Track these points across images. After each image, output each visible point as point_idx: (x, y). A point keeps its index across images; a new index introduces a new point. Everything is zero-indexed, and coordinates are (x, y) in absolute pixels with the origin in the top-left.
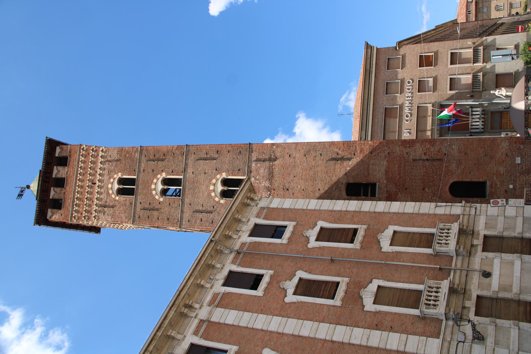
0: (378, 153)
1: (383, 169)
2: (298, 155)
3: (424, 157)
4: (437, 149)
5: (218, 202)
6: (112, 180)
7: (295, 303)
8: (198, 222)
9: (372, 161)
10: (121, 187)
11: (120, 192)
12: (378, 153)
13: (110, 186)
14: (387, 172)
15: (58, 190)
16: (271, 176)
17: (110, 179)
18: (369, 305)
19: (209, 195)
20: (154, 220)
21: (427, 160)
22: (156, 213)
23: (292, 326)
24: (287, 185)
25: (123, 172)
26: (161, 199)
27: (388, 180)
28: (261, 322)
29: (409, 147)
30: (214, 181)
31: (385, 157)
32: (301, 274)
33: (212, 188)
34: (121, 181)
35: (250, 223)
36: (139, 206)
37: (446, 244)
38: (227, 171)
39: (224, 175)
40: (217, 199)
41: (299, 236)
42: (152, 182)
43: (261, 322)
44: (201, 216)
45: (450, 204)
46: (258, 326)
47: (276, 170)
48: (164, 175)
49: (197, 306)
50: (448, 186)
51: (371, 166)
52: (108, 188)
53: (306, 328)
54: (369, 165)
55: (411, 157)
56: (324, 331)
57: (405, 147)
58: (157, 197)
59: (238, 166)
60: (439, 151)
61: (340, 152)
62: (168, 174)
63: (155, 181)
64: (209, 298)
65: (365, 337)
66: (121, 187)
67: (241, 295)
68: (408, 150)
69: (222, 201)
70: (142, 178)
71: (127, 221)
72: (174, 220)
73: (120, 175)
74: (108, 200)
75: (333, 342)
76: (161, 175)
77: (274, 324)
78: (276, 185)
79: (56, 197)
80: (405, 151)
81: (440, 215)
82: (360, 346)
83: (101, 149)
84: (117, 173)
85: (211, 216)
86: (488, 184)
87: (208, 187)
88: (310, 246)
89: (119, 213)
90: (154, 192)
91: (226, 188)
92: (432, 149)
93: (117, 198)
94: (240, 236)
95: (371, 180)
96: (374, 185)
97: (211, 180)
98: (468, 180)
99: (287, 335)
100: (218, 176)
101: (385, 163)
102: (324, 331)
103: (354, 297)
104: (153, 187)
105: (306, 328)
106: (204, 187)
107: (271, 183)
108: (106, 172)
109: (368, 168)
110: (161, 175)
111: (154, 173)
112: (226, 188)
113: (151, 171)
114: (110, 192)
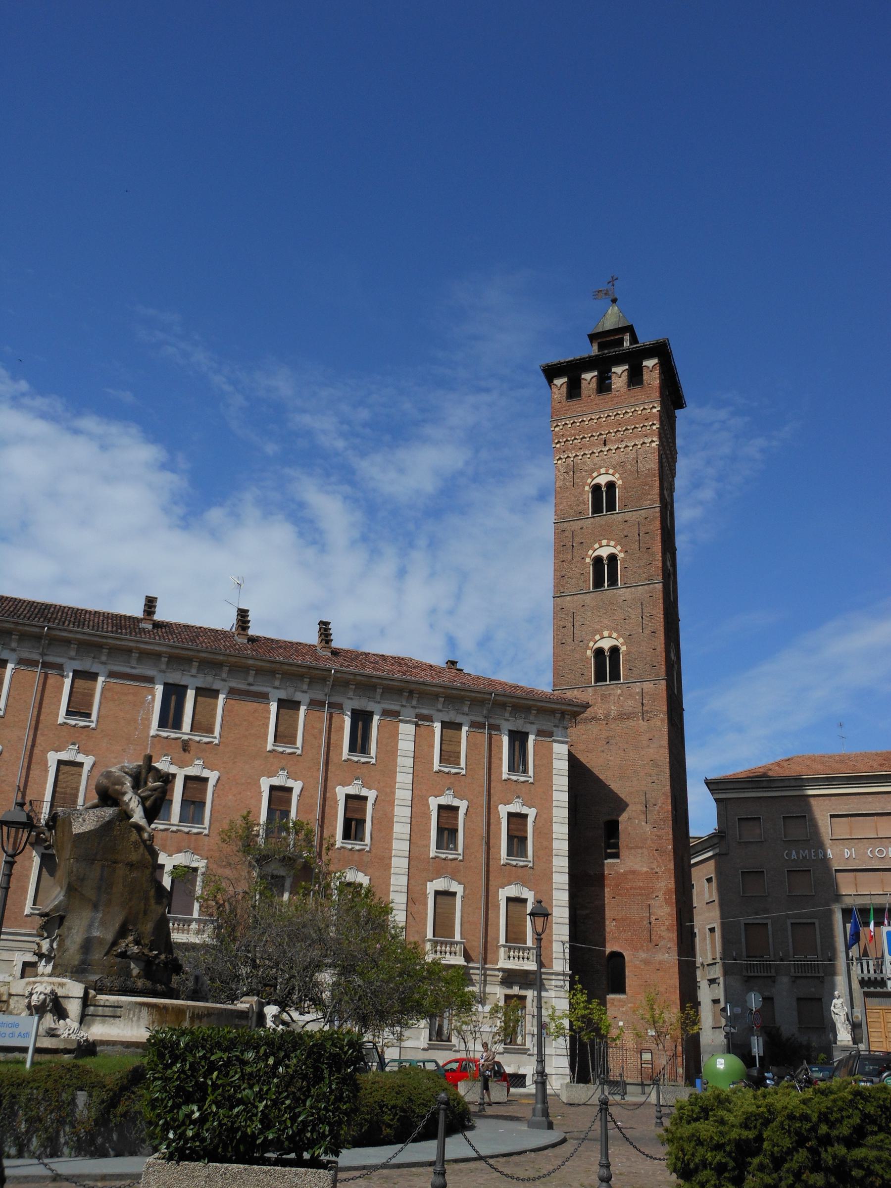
0: (656, 859)
1: (637, 867)
2: (651, 751)
3: (653, 918)
4: (663, 934)
5: (587, 647)
6: (611, 471)
7: (429, 808)
8: (562, 623)
9: (645, 851)
10: (604, 489)
11: (596, 488)
12: (656, 859)
13: (603, 471)
14: (633, 872)
15: (594, 384)
16: (624, 717)
17: (613, 467)
18: (432, 887)
19: (597, 632)
20: (561, 556)
21: (650, 923)
22: (569, 556)
23: (402, 813)
24: (612, 741)
25: (624, 488)
26: (588, 560)
27: (625, 874)
28: (404, 779)
29: (665, 898)
30: (615, 635)
31: (652, 869)
32: (463, 805)
33: (606, 634)
34: (611, 486)
35: (528, 725)
36: (576, 525)
37: (509, 957)
38: (628, 653)
39: (623, 648)
40: (591, 644)
41: (513, 790)
42: (609, 539)
43: (404, 779)
44: (569, 625)
45: (567, 957)
46: (400, 778)
47: (631, 723)
48: (621, 555)
49: (414, 703)
50: (620, 950)
51: (640, 851)
52: (600, 467)
53: (401, 828)
54: (641, 848)
55: (652, 902)
56: (400, 847)
57: (665, 894)
58: (590, 552)
59: (635, 666)
60: (660, 937)
61: (657, 808)
62: (623, 561)
63: (612, 543)
64: (425, 712)
65: (398, 889)
66: (604, 489)
67: (433, 747)
68: (661, 897)
69: (589, 653)
70: (616, 517)
71: (558, 512)
72: (562, 586)
73: (619, 482)
74: (584, 474)
75: (390, 858)
76: (620, 552)
77: (403, 795)
78: (613, 726)
79: (584, 384)
80: (661, 894)
81: (552, 947)
82: (389, 885)
83: (654, 439)
84: (620, 478)
85: (570, 640)
86: (622, 996)
87: (607, 628)
88: (501, 807)
89: (567, 498)
90: (596, 546)
91: (607, 654)
92: (662, 928)
93: (587, 488)
94: (508, 720)
95: (623, 852)
96: (616, 856)
97: (616, 631)
98: (627, 973)
99: (393, 810)
100: (621, 640)
101: (645, 869)
102: (400, 847)
103: (440, 869)
104: (604, 542)
105: (401, 828)
106: (606, 621)
107: (615, 719)
108: (623, 458)
109: (637, 847)
110: (620, 552)
111: (624, 540)
112: (607, 654)
113: (625, 533)
114: (595, 474)
